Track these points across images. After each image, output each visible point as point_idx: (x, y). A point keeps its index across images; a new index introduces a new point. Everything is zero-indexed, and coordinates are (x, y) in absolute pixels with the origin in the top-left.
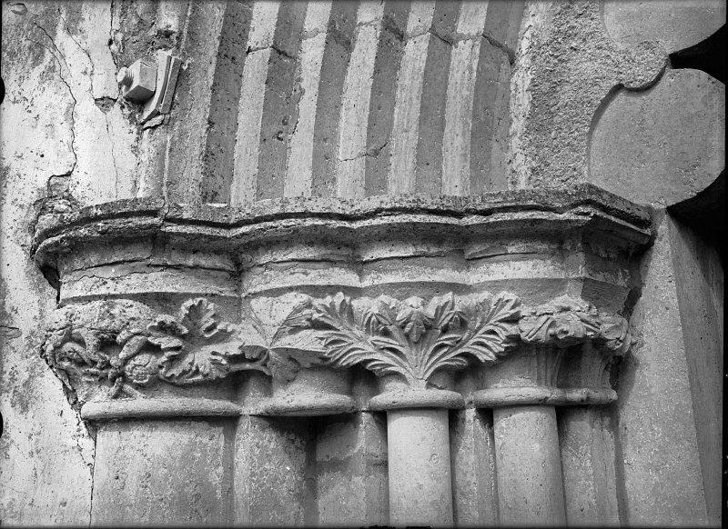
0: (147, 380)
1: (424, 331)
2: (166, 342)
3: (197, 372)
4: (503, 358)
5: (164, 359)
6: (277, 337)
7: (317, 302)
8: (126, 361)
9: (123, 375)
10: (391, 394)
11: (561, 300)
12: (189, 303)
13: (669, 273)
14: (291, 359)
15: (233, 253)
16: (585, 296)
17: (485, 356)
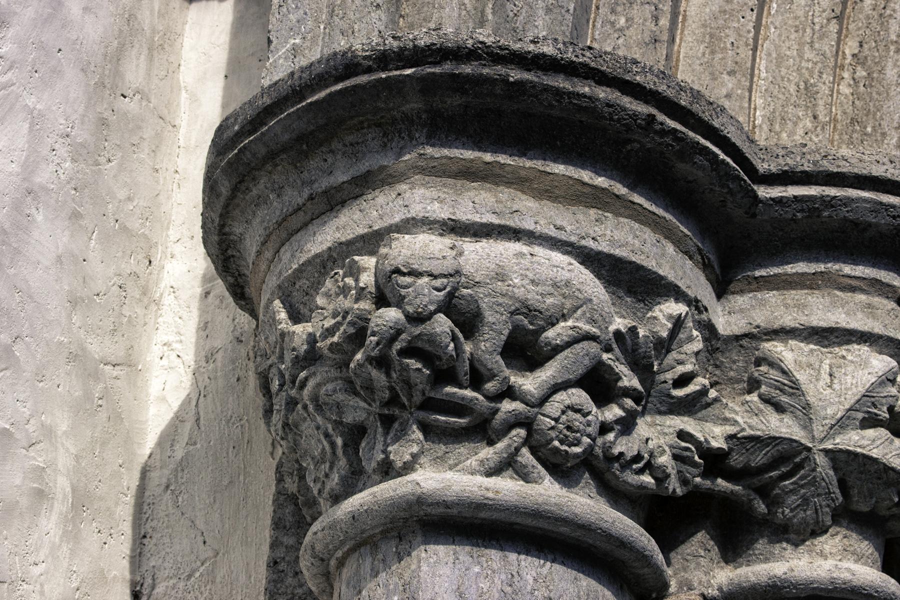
0: (577, 450)
3: (649, 467)
5: (613, 412)
6: (841, 425)
8: (557, 388)
9: (527, 423)
14: (843, 484)
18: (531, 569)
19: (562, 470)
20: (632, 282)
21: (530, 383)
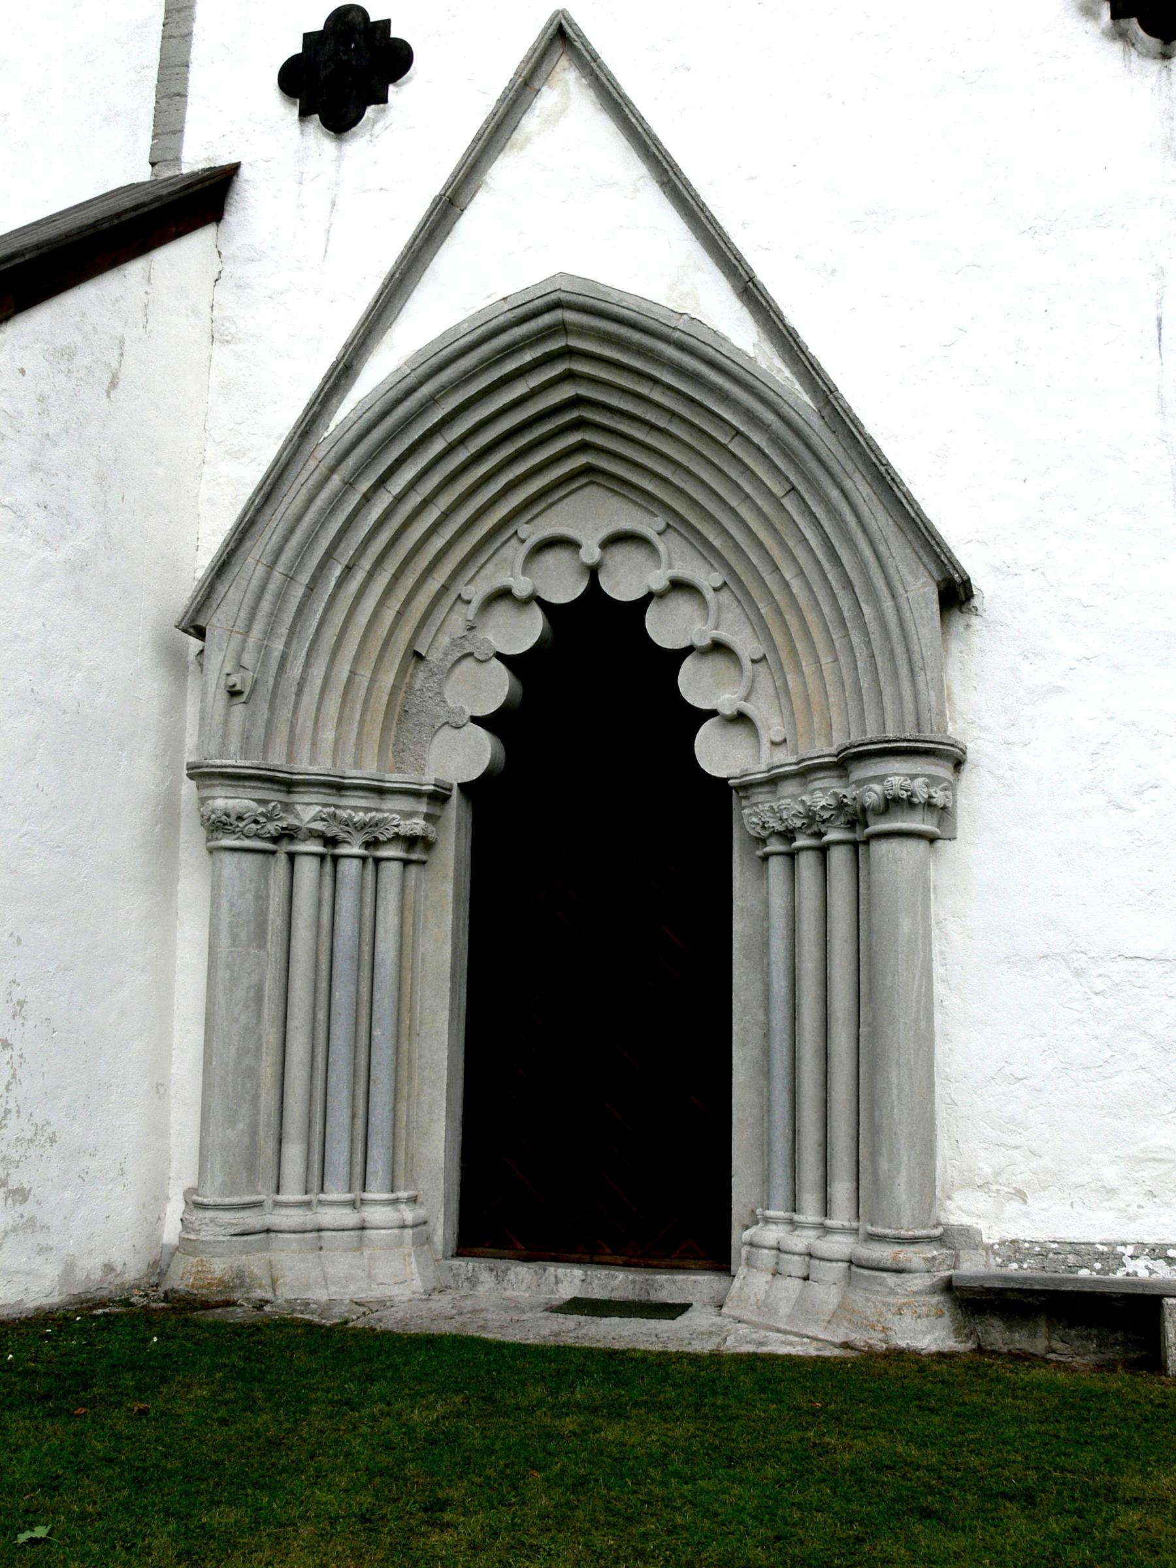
2: (262, 820)
4: (389, 840)
7: (325, 810)
11: (415, 820)
12: (273, 804)
13: (455, 812)
15: (289, 786)
16: (424, 819)
17: (382, 838)
21: (241, 825)
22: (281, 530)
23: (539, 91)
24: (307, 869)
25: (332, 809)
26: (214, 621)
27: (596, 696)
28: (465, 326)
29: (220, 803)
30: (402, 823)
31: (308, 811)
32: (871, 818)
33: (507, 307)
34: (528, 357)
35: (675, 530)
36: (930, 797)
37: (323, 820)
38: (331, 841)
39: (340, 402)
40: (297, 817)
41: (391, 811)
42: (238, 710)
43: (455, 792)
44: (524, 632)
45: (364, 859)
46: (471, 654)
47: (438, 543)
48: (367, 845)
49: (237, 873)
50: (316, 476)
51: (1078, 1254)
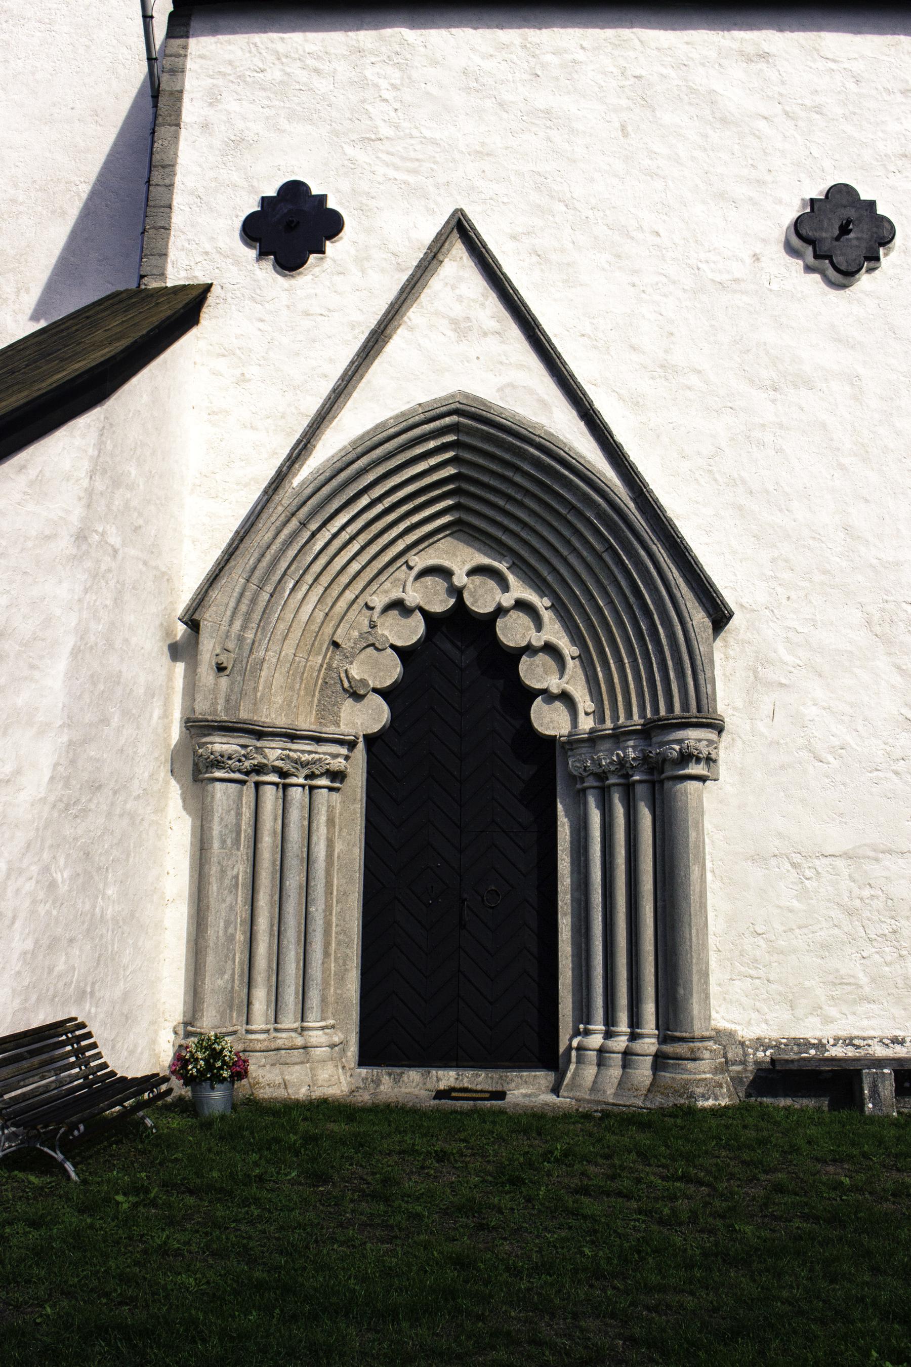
1: (305, 765)
2: (243, 759)
10: (293, 780)
17: (317, 772)
18: (229, 784)
19: (234, 772)
20: (244, 747)
22: (256, 555)
23: (442, 262)
24: (270, 795)
25: (287, 752)
26: (207, 616)
27: (456, 674)
28: (392, 421)
29: (217, 747)
30: (332, 762)
31: (274, 752)
32: (667, 766)
33: (421, 411)
34: (432, 444)
35: (518, 566)
36: (710, 754)
37: (282, 759)
38: (283, 774)
39: (301, 466)
40: (265, 757)
41: (325, 754)
42: (224, 681)
43: (361, 739)
44: (412, 631)
45: (303, 786)
46: (373, 645)
47: (355, 566)
48: (306, 777)
49: (224, 798)
50: (283, 518)
51: (799, 1045)
